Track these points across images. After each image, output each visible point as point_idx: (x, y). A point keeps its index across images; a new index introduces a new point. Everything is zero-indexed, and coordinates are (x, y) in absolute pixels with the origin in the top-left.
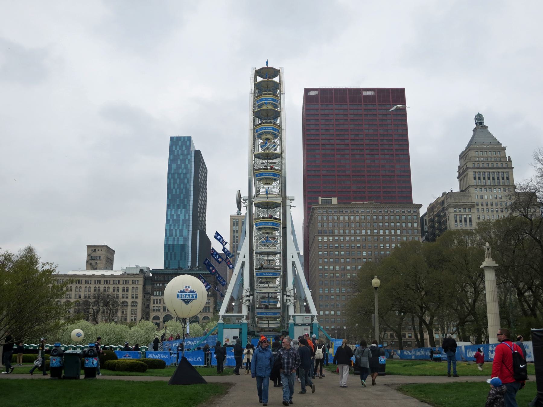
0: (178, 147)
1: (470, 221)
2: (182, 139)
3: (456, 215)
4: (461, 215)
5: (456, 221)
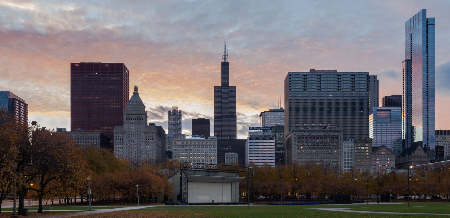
0: (2, 97)
1: (123, 139)
2: (4, 92)
3: (116, 136)
4: (118, 136)
5: (116, 139)
